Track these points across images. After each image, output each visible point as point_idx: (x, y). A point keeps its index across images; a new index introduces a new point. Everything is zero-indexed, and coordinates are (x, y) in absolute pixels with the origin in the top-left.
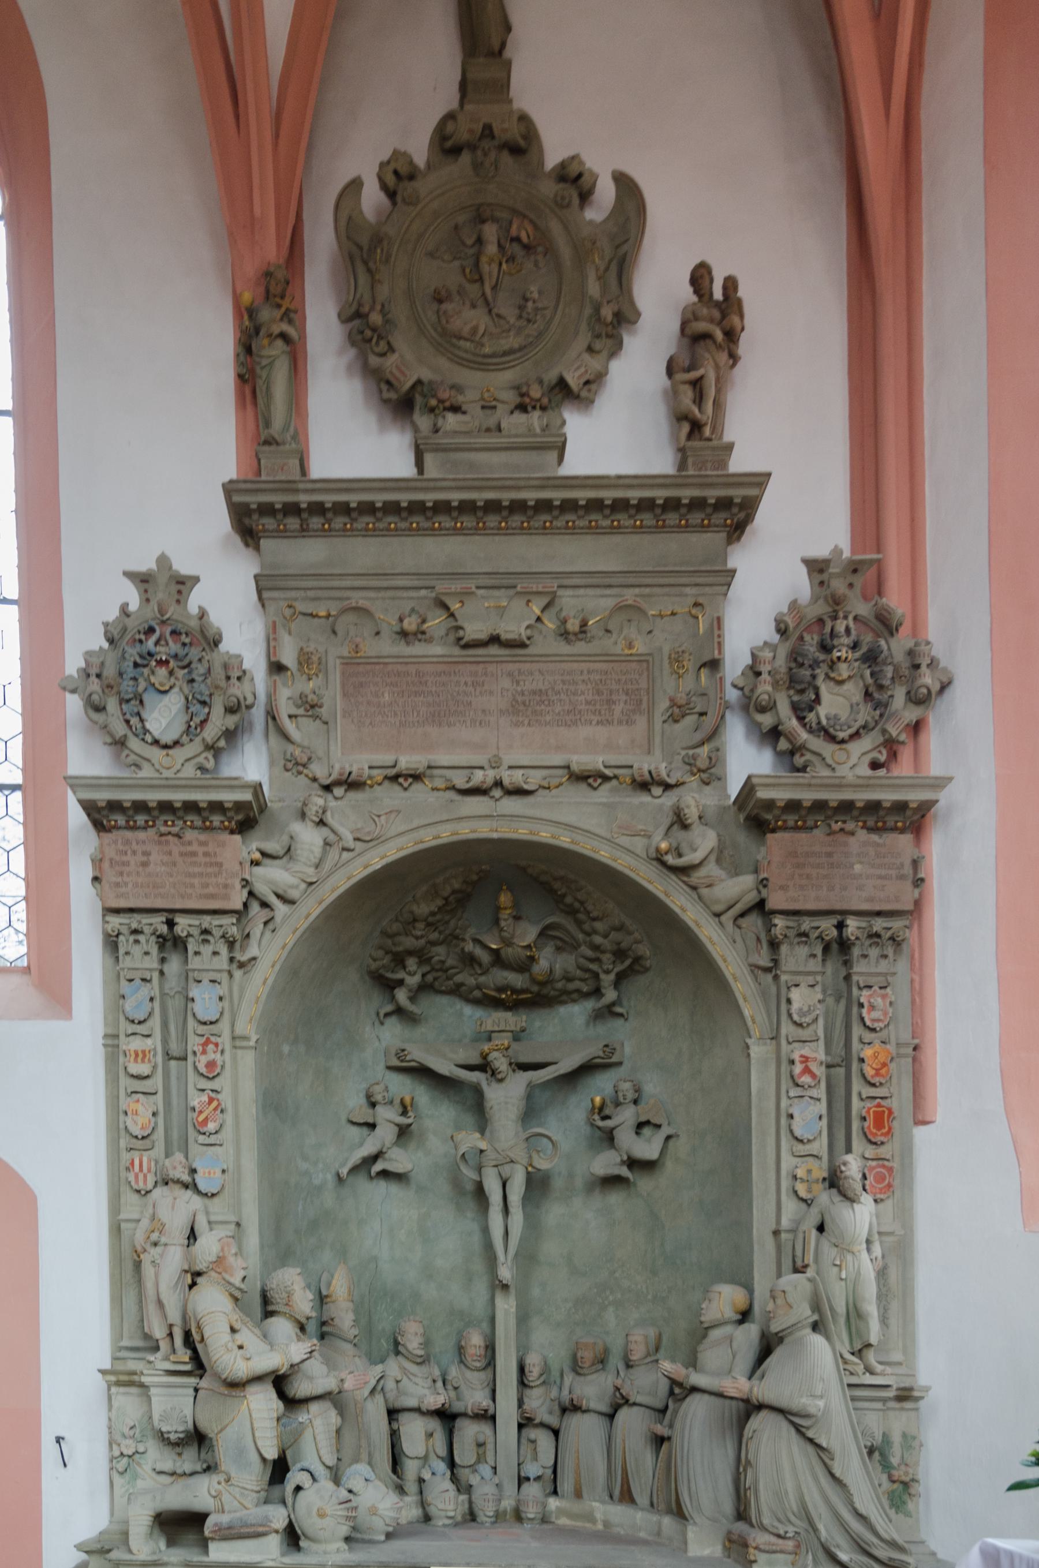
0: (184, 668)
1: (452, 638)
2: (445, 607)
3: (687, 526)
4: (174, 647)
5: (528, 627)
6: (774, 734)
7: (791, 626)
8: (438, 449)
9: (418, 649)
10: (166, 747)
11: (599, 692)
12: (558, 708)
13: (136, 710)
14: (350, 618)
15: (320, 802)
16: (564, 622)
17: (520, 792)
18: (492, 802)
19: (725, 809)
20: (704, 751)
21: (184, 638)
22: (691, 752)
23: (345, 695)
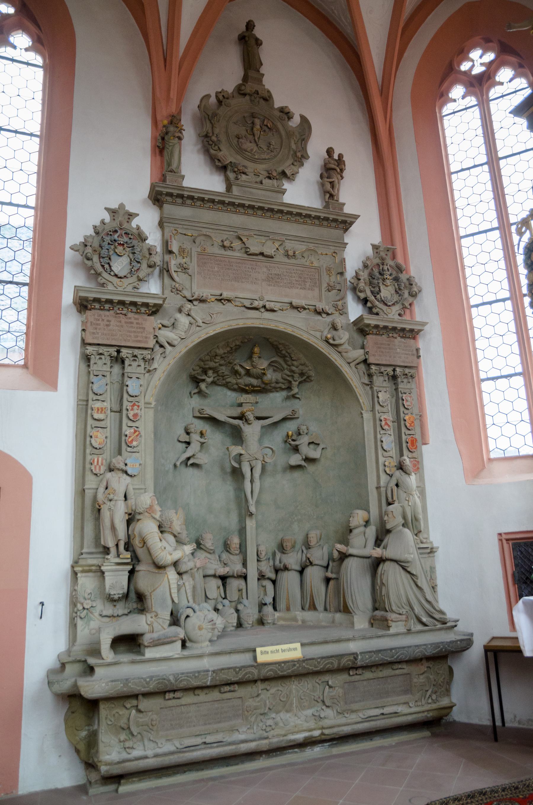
0: (129, 247)
1: (243, 250)
2: (241, 240)
3: (330, 226)
4: (126, 239)
5: (274, 251)
6: (365, 301)
7: (369, 265)
8: (238, 185)
9: (229, 253)
10: (121, 278)
11: (300, 277)
12: (285, 281)
13: (107, 262)
14: (202, 238)
15: (189, 306)
16: (287, 251)
17: (273, 311)
18: (260, 313)
19: (349, 324)
20: (340, 303)
21: (130, 236)
22: (335, 303)
23: (198, 266)
